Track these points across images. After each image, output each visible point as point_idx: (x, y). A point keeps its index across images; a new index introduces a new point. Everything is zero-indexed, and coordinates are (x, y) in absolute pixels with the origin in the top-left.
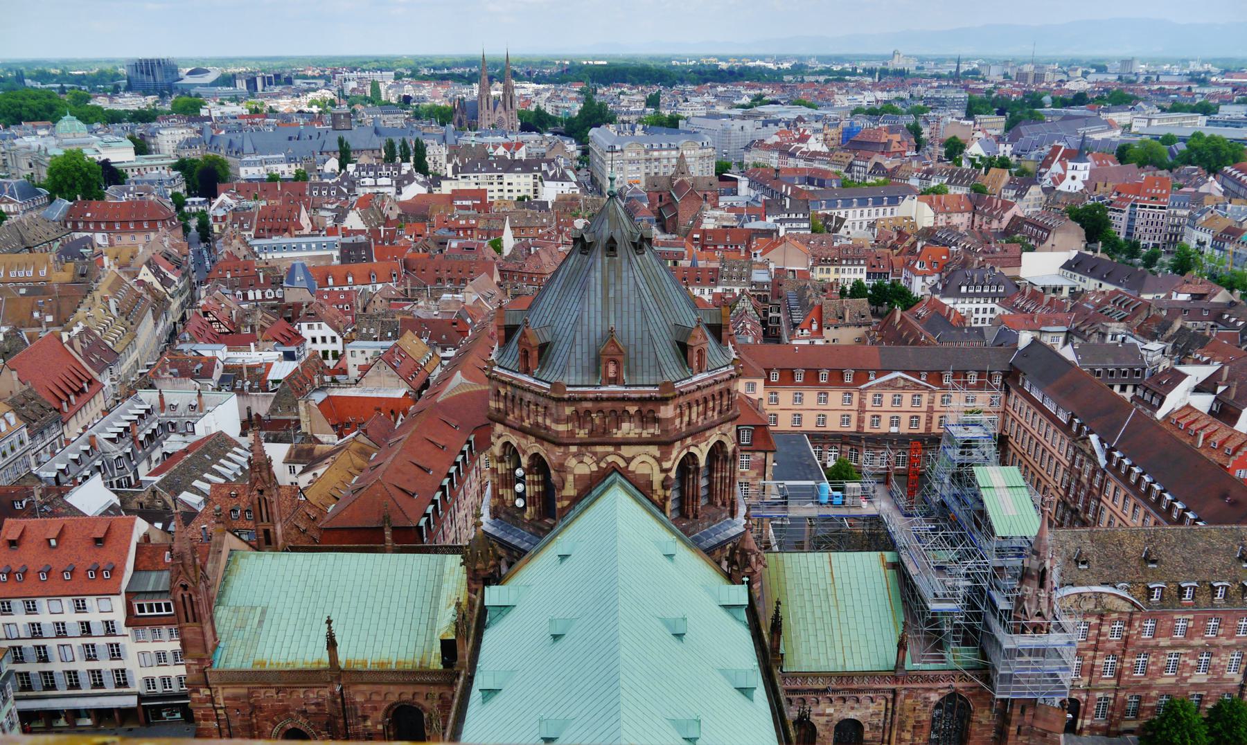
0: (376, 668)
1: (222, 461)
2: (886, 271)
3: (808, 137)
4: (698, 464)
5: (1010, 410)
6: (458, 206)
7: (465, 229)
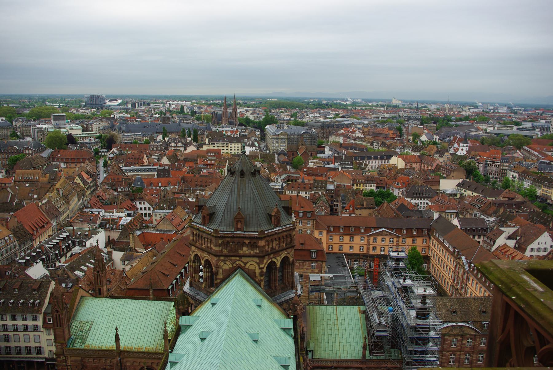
0: (136, 350)
2: (384, 186)
3: (355, 131)
5: (431, 245)
7: (210, 165)
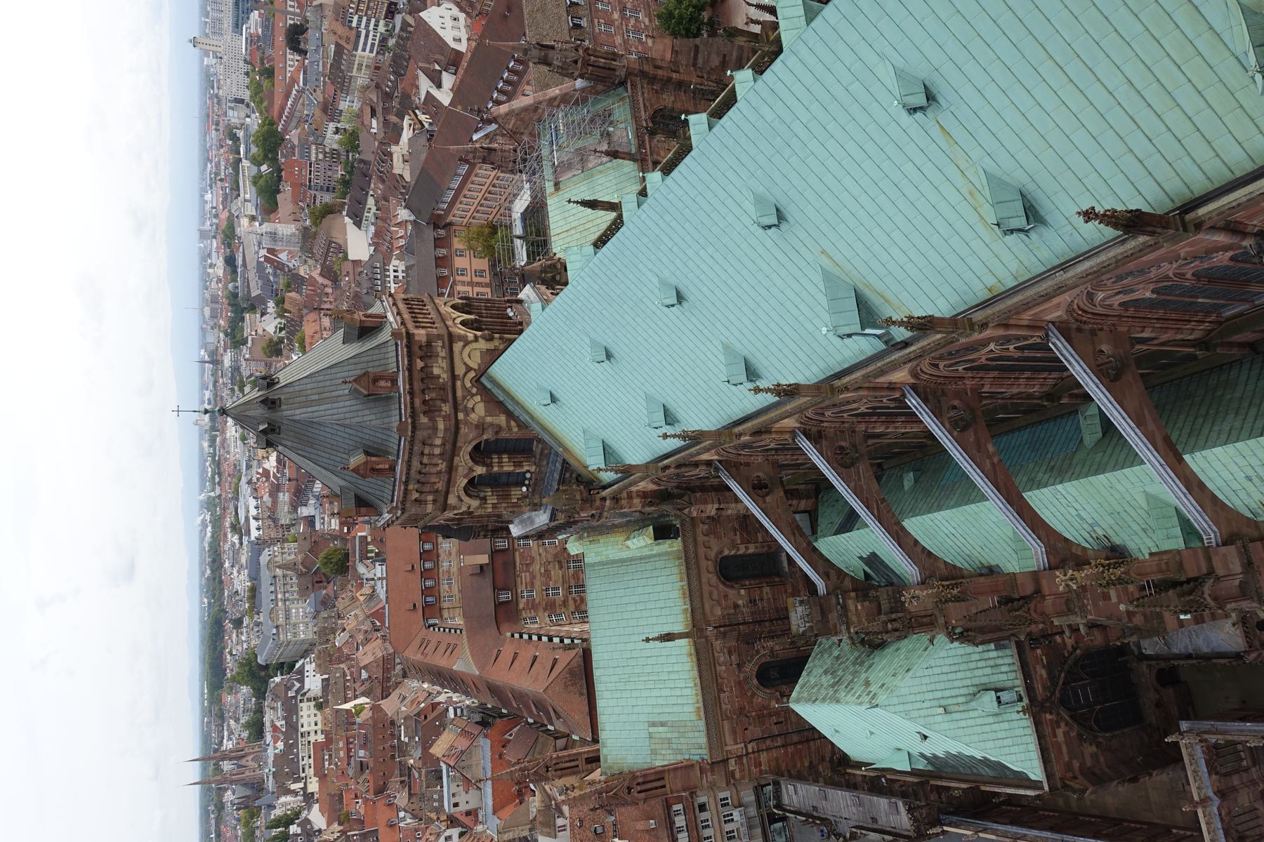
3: (265, 470)
4: (472, 320)
5: (465, 220)
7: (349, 750)
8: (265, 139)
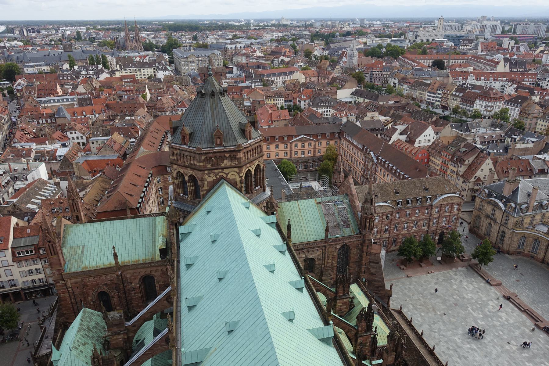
1: (43, 190)
2: (291, 99)
4: (252, 173)
5: (342, 146)
6: (124, 82)
7: (129, 91)
8: (395, 51)
